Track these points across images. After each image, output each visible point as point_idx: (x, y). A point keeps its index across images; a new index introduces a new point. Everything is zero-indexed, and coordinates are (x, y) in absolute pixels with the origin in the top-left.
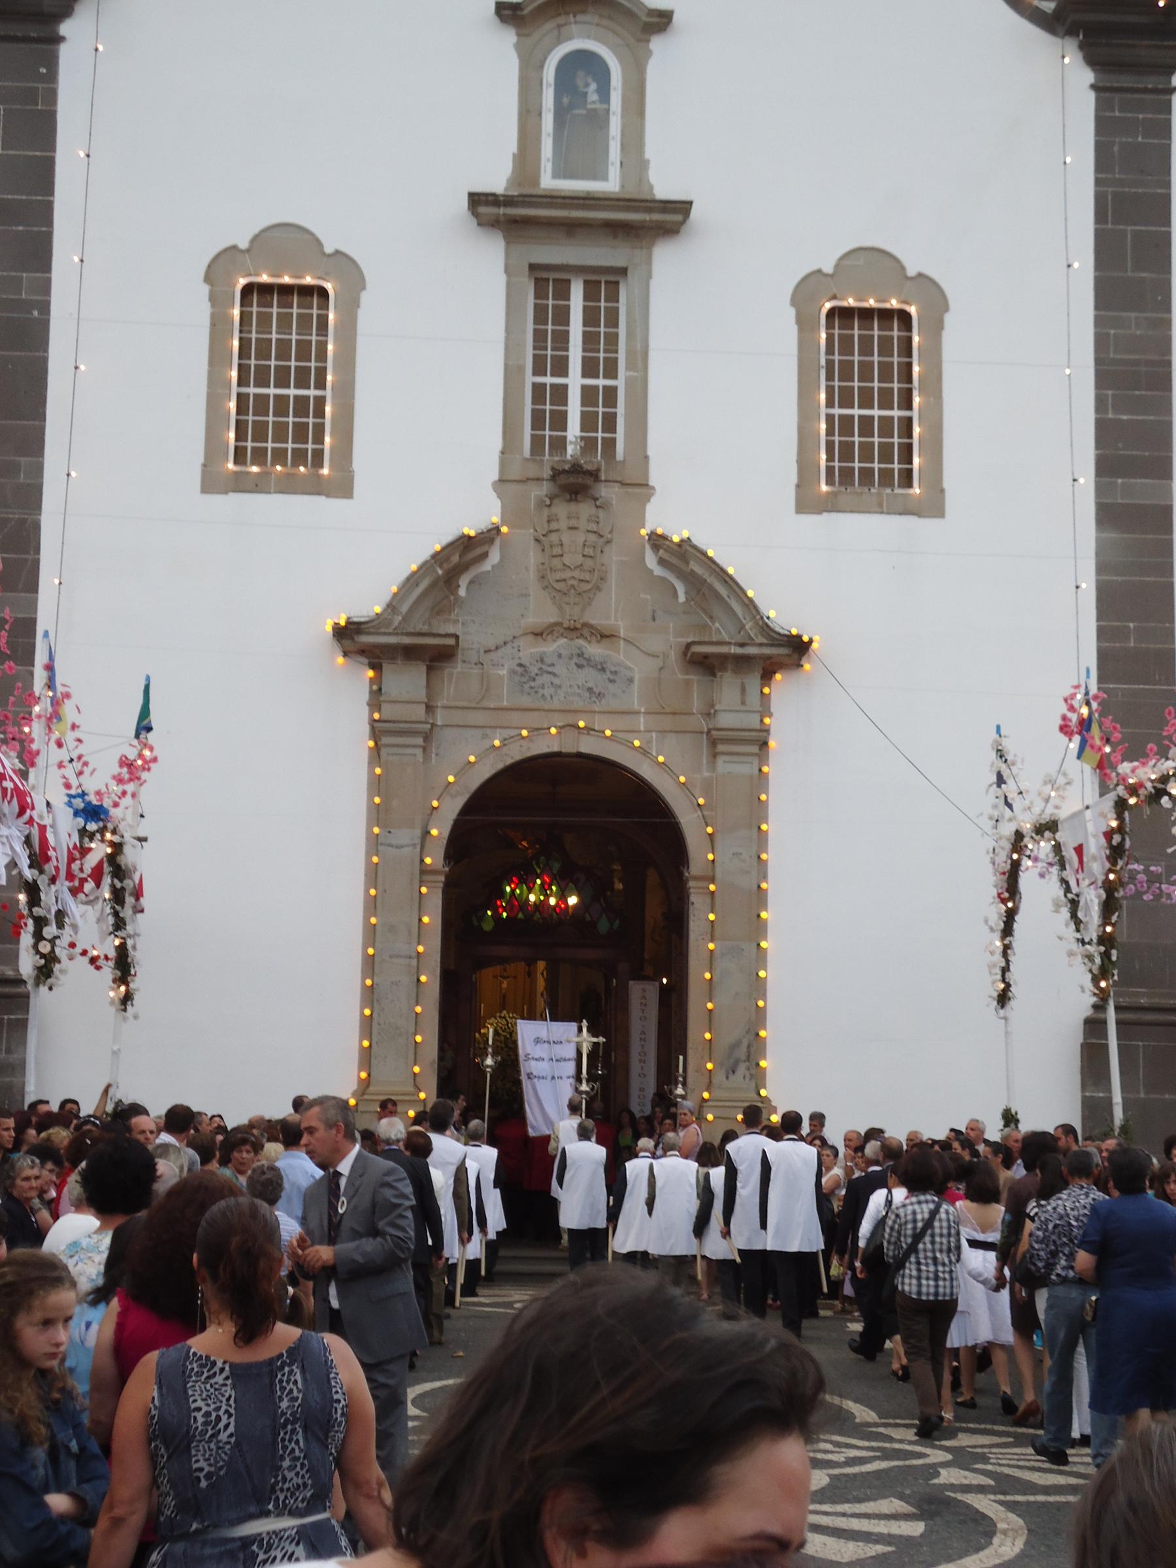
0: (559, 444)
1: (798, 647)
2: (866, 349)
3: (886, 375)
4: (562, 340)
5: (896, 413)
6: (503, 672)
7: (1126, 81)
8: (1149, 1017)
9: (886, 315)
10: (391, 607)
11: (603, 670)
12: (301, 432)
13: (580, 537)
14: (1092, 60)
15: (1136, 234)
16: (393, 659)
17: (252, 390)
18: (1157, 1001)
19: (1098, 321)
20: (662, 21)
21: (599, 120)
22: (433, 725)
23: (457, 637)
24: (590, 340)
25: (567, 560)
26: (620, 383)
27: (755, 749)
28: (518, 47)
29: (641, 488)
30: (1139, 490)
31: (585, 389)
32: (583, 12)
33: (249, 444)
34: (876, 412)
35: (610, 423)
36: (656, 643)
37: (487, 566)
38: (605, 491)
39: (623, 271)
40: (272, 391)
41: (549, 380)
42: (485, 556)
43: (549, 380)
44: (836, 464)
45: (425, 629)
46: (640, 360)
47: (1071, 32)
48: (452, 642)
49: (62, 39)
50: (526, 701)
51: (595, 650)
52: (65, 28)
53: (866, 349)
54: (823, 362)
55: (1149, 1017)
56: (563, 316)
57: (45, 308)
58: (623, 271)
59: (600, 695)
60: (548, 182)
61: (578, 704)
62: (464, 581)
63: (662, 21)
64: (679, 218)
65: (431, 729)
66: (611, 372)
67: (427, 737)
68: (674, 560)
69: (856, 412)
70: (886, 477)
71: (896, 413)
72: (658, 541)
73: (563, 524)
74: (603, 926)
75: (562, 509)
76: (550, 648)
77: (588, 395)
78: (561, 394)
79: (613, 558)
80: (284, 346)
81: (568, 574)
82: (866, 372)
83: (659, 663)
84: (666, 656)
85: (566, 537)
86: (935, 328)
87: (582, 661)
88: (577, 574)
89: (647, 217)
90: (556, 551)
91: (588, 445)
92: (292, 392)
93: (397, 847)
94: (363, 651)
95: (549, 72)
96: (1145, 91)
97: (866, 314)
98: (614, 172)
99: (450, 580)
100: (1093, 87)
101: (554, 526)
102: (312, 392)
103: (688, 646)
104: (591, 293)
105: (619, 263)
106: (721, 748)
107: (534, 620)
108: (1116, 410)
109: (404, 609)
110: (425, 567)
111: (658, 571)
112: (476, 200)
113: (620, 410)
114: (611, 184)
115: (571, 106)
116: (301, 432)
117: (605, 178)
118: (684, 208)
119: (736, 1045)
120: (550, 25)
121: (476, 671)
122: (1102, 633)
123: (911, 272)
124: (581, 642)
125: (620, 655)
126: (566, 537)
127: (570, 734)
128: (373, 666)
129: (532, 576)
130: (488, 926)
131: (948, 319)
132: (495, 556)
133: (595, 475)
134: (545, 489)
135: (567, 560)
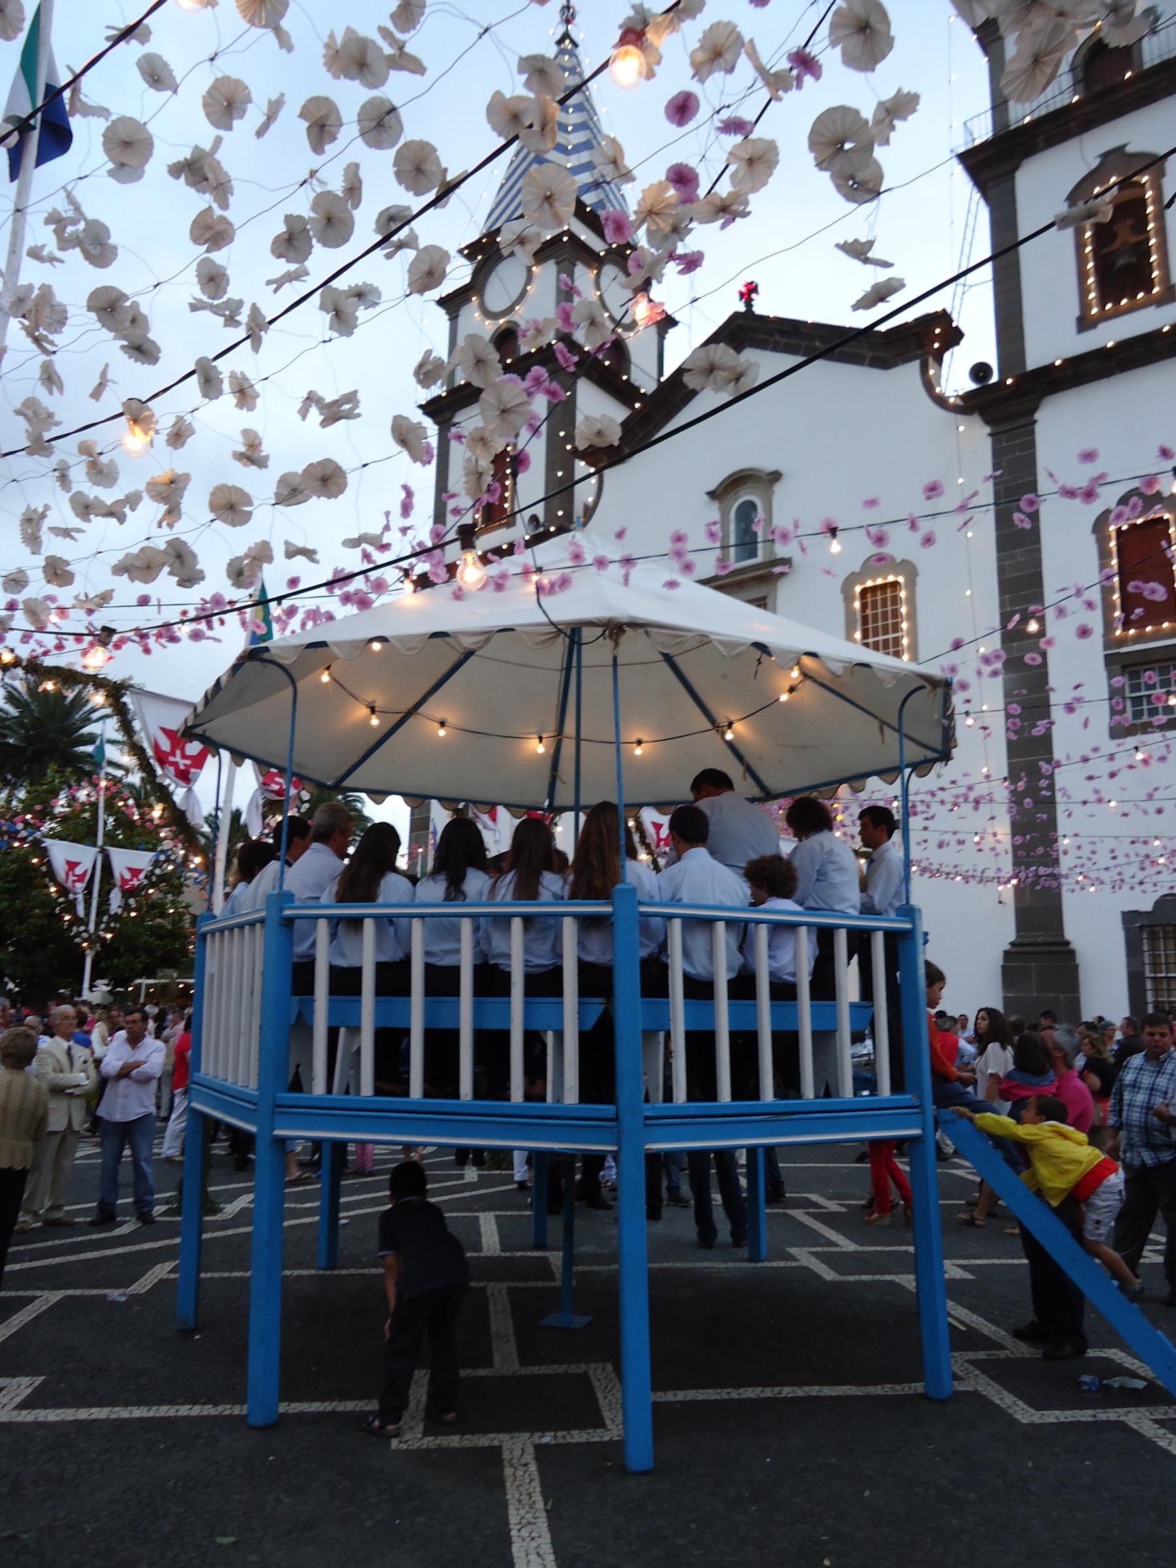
7: (1006, 426)
8: (1038, 949)
14: (987, 421)
19: (999, 560)
20: (776, 476)
28: (719, 509)
39: (765, 598)
53: (884, 604)
54: (859, 617)
55: (1047, 948)
58: (765, 598)
63: (776, 476)
86: (911, 585)
95: (732, 516)
98: (760, 552)
100: (990, 435)
105: (762, 594)
114: (759, 559)
117: (755, 555)
123: (898, 560)
131: (919, 580)
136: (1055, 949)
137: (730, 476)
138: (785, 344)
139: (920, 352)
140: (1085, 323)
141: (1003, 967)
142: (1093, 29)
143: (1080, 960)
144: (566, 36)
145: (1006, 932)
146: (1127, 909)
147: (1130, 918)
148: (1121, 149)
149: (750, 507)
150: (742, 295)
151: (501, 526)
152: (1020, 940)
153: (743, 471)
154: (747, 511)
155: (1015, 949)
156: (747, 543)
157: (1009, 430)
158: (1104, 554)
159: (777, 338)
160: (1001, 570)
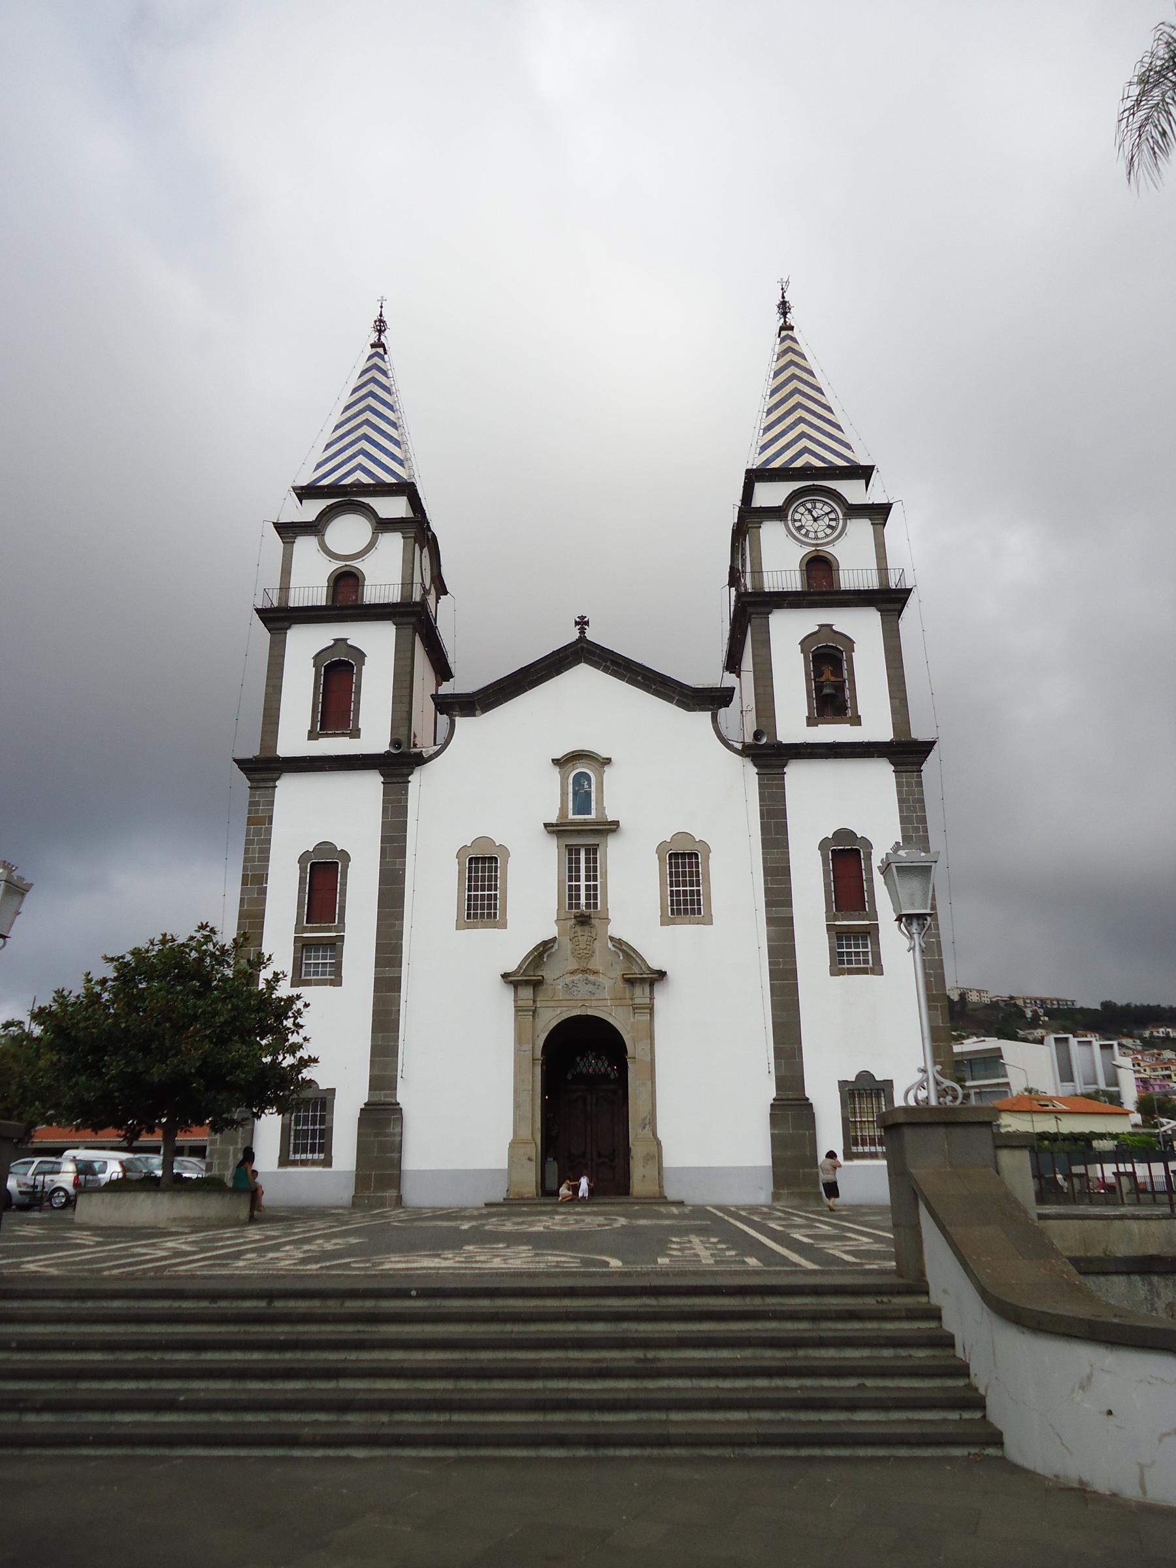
0: (578, 906)
1: (662, 974)
2: (684, 867)
3: (691, 875)
4: (578, 869)
5: (695, 888)
6: (560, 987)
8: (793, 1102)
9: (691, 855)
10: (520, 967)
11: (595, 985)
12: (489, 907)
13: (585, 938)
14: (755, 765)
15: (776, 823)
16: (521, 985)
17: (473, 893)
18: (796, 1097)
19: (763, 853)
21: (588, 794)
22: (536, 1007)
23: (543, 976)
24: (588, 869)
25: (581, 946)
26: (598, 883)
27: (648, 1011)
28: (559, 772)
29: (606, 920)
30: (780, 912)
31: (586, 885)
32: (581, 759)
33: (472, 912)
34: (688, 888)
35: (595, 898)
36: (613, 976)
37: (553, 950)
38: (593, 921)
40: (479, 893)
41: (574, 883)
42: (552, 946)
43: (574, 883)
44: (675, 907)
45: (532, 974)
46: (604, 875)
47: (747, 756)
48: (541, 978)
49: (410, 782)
50: (568, 997)
51: (592, 978)
52: (410, 778)
53: (684, 867)
55: (793, 1102)
56: (578, 861)
57: (404, 870)
59: (594, 994)
60: (571, 816)
61: (587, 997)
62: (545, 956)
63: (608, 761)
64: (615, 827)
65: (535, 1010)
66: (595, 879)
67: (534, 1012)
68: (617, 945)
69: (681, 888)
70: (693, 912)
71: (695, 888)
72: (612, 939)
73: (579, 934)
74: (612, 1076)
75: (578, 928)
76: (576, 977)
77: (588, 887)
78: (578, 888)
79: (597, 944)
80: (483, 877)
81: (581, 951)
82: (684, 875)
83: (614, 981)
84: (616, 978)
85: (580, 938)
87: (587, 982)
88: (585, 951)
89: (604, 827)
90: (577, 943)
91: (588, 905)
92: (486, 893)
93: (525, 1051)
94: (511, 982)
96: (775, 774)
97: (683, 855)
98: (593, 811)
99: (541, 955)
101: (576, 935)
102: (493, 892)
103: (624, 974)
104: (587, 852)
106: (636, 1011)
107: (571, 968)
108: (771, 884)
109: (524, 967)
110: (531, 953)
111: (613, 949)
112: (546, 825)
113: (599, 892)
114: (593, 816)
115: (579, 790)
116: (489, 907)
118: (617, 823)
119: (646, 1118)
120: (569, 765)
121: (551, 987)
122: (770, 963)
123: (697, 840)
124: (586, 975)
125: (601, 979)
126: (580, 938)
127: (583, 1008)
128: (516, 987)
129: (569, 952)
130: (569, 1077)
132: (556, 946)
133: (589, 917)
134: (573, 921)
135: (581, 946)
136: (802, 1102)
137: (573, 752)
138: (613, 670)
139: (711, 707)
140: (811, 722)
141: (771, 1114)
142: (814, 549)
143: (817, 1109)
144: (378, 344)
145: (771, 1092)
146: (841, 1080)
147: (843, 1084)
148: (830, 626)
149: (589, 779)
150: (577, 623)
151: (343, 735)
152: (779, 1097)
153: (583, 751)
154: (581, 778)
155: (777, 1103)
156: (583, 802)
157: (766, 774)
158: (825, 863)
159: (608, 664)
160: (765, 860)
